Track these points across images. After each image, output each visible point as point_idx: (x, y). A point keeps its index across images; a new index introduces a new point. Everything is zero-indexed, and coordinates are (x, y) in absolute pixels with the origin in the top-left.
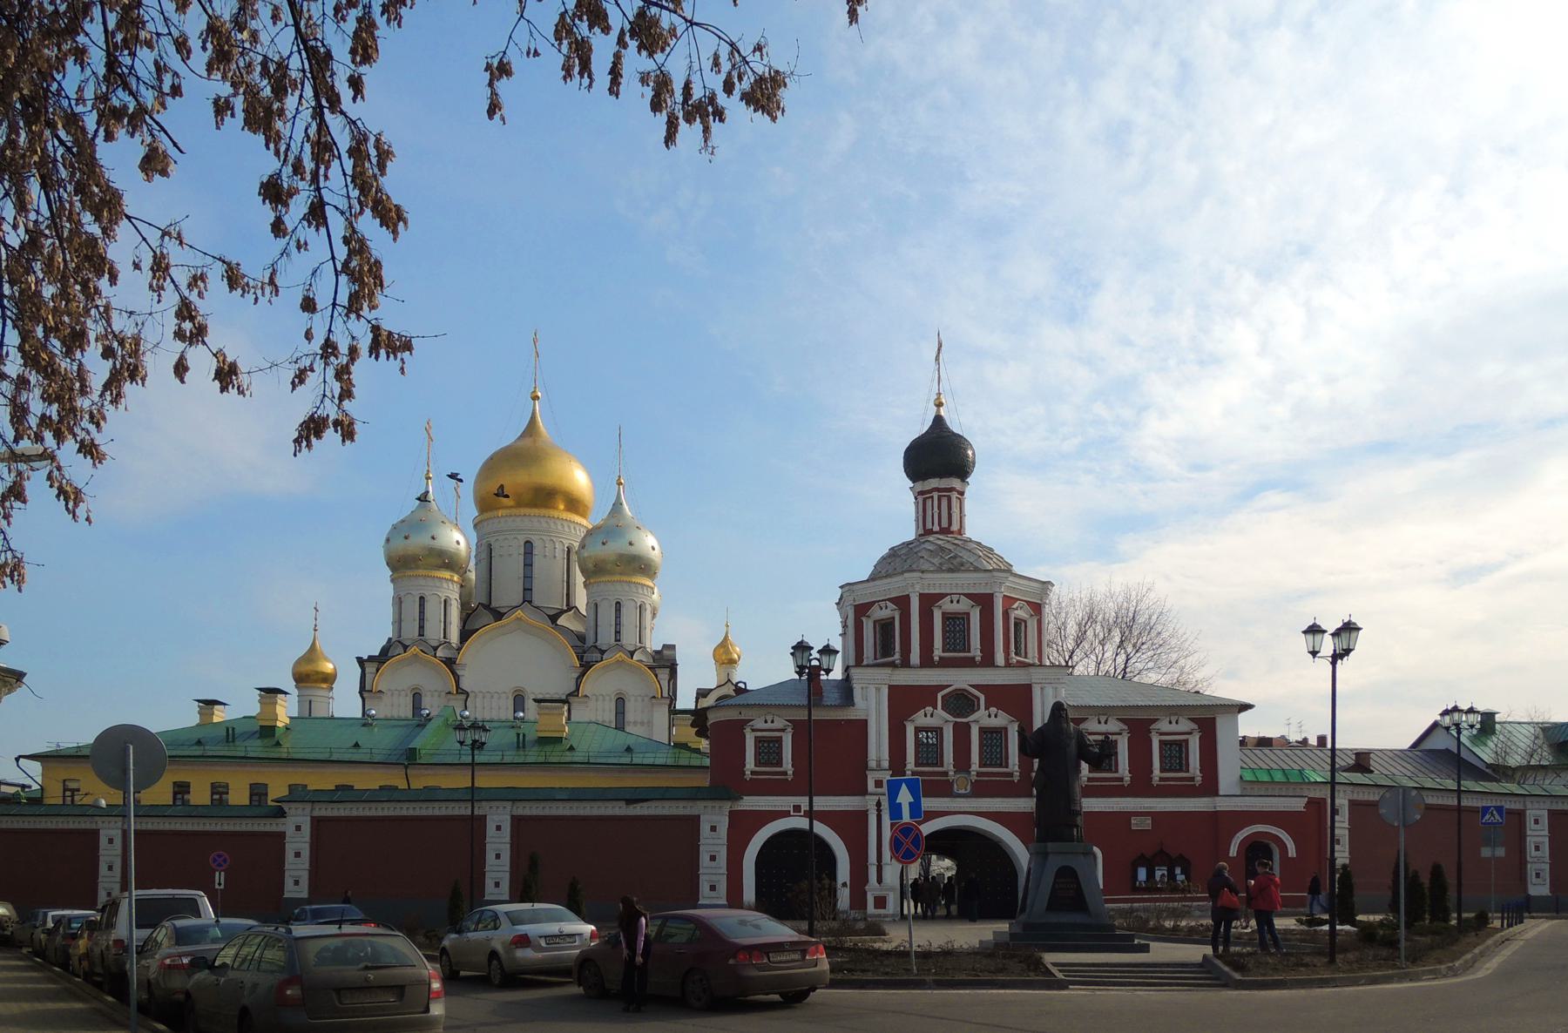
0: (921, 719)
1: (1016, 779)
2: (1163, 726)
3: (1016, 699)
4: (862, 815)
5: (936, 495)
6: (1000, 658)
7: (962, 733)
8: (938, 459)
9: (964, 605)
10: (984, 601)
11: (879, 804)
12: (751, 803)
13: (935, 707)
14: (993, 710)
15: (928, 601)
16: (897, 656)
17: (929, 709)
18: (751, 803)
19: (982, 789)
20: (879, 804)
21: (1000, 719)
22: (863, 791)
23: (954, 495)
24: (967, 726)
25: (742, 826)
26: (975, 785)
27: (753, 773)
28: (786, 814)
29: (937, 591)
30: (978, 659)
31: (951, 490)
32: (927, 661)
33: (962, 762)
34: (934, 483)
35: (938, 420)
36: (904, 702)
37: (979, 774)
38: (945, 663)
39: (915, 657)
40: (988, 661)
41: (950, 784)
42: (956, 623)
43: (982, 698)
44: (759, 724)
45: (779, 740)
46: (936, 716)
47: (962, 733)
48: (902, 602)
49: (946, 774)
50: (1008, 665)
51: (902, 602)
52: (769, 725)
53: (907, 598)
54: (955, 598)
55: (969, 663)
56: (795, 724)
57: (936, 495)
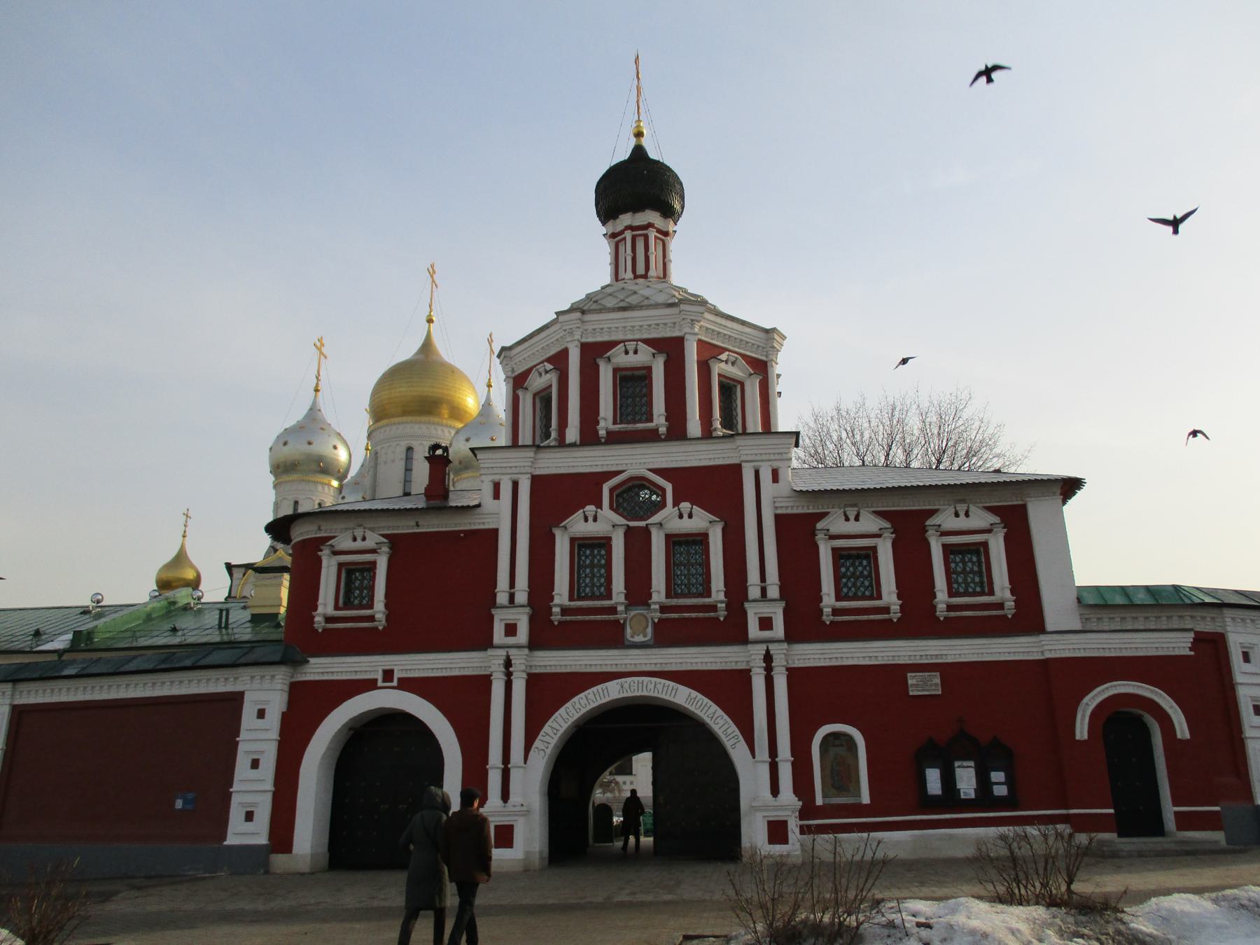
0: (579, 525)
1: (722, 614)
2: (946, 520)
3: (717, 489)
4: (484, 682)
5: (628, 235)
6: (694, 426)
7: (638, 543)
8: (638, 192)
9: (644, 356)
10: (671, 349)
11: (508, 663)
12: (322, 668)
13: (599, 506)
14: (685, 506)
15: (593, 352)
16: (554, 435)
17: (590, 509)
18: (322, 668)
19: (670, 633)
20: (508, 663)
21: (699, 520)
22: (484, 642)
23: (652, 234)
24: (646, 533)
25: (306, 707)
26: (659, 627)
27: (329, 619)
28: (370, 685)
29: (606, 338)
30: (663, 430)
31: (650, 225)
32: (589, 437)
33: (638, 591)
34: (626, 219)
35: (639, 152)
36: (555, 498)
37: (663, 609)
38: (615, 439)
39: (572, 434)
40: (677, 431)
41: (619, 627)
42: (633, 383)
43: (669, 487)
44: (344, 543)
45: (372, 566)
46: (603, 521)
47: (638, 543)
48: (559, 361)
49: (613, 610)
50: (708, 434)
51: (559, 361)
52: (359, 545)
53: (564, 354)
54: (631, 346)
55: (651, 437)
56: (395, 541)
57: (628, 235)
